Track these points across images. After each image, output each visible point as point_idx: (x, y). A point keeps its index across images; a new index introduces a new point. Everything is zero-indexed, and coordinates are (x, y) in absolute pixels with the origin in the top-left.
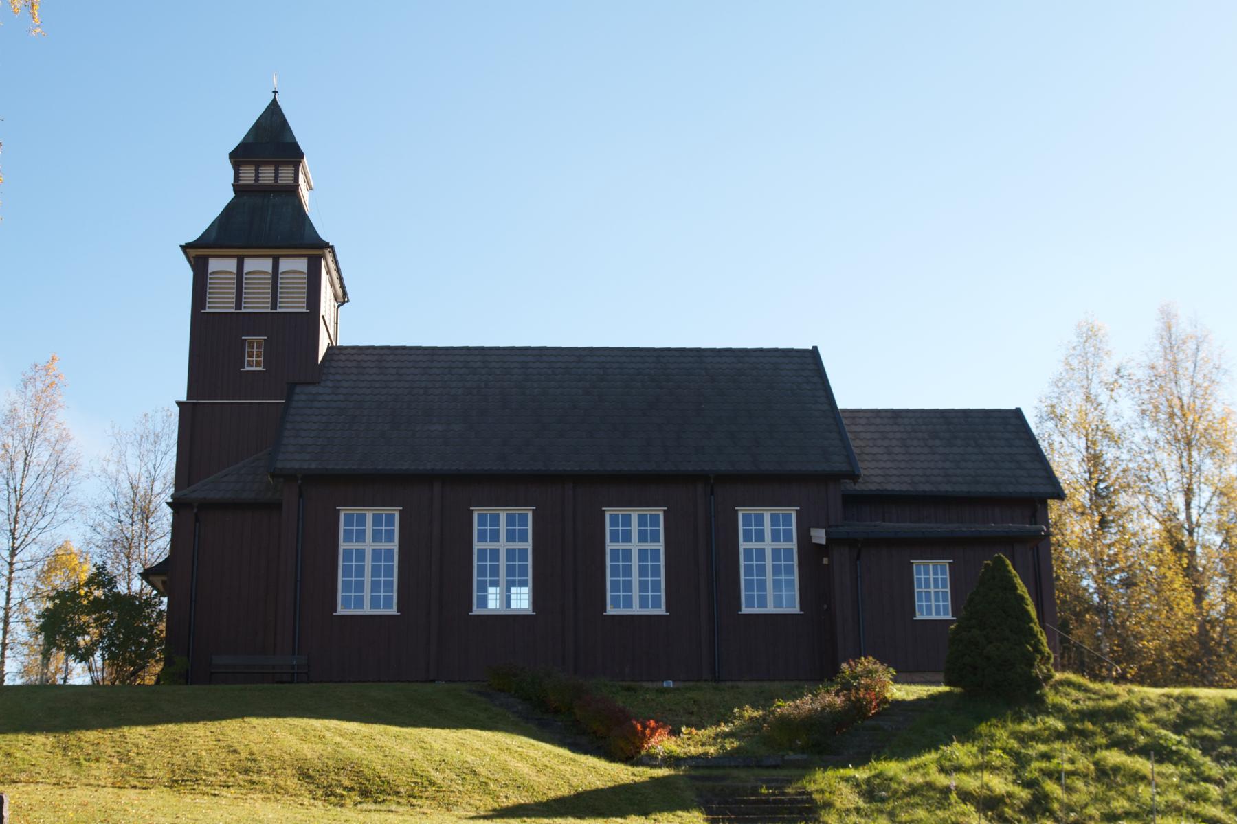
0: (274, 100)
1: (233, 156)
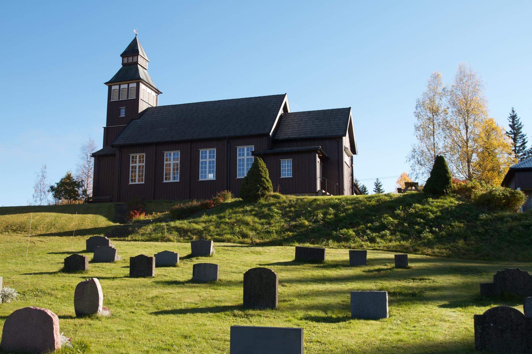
0: (136, 38)
1: (121, 55)
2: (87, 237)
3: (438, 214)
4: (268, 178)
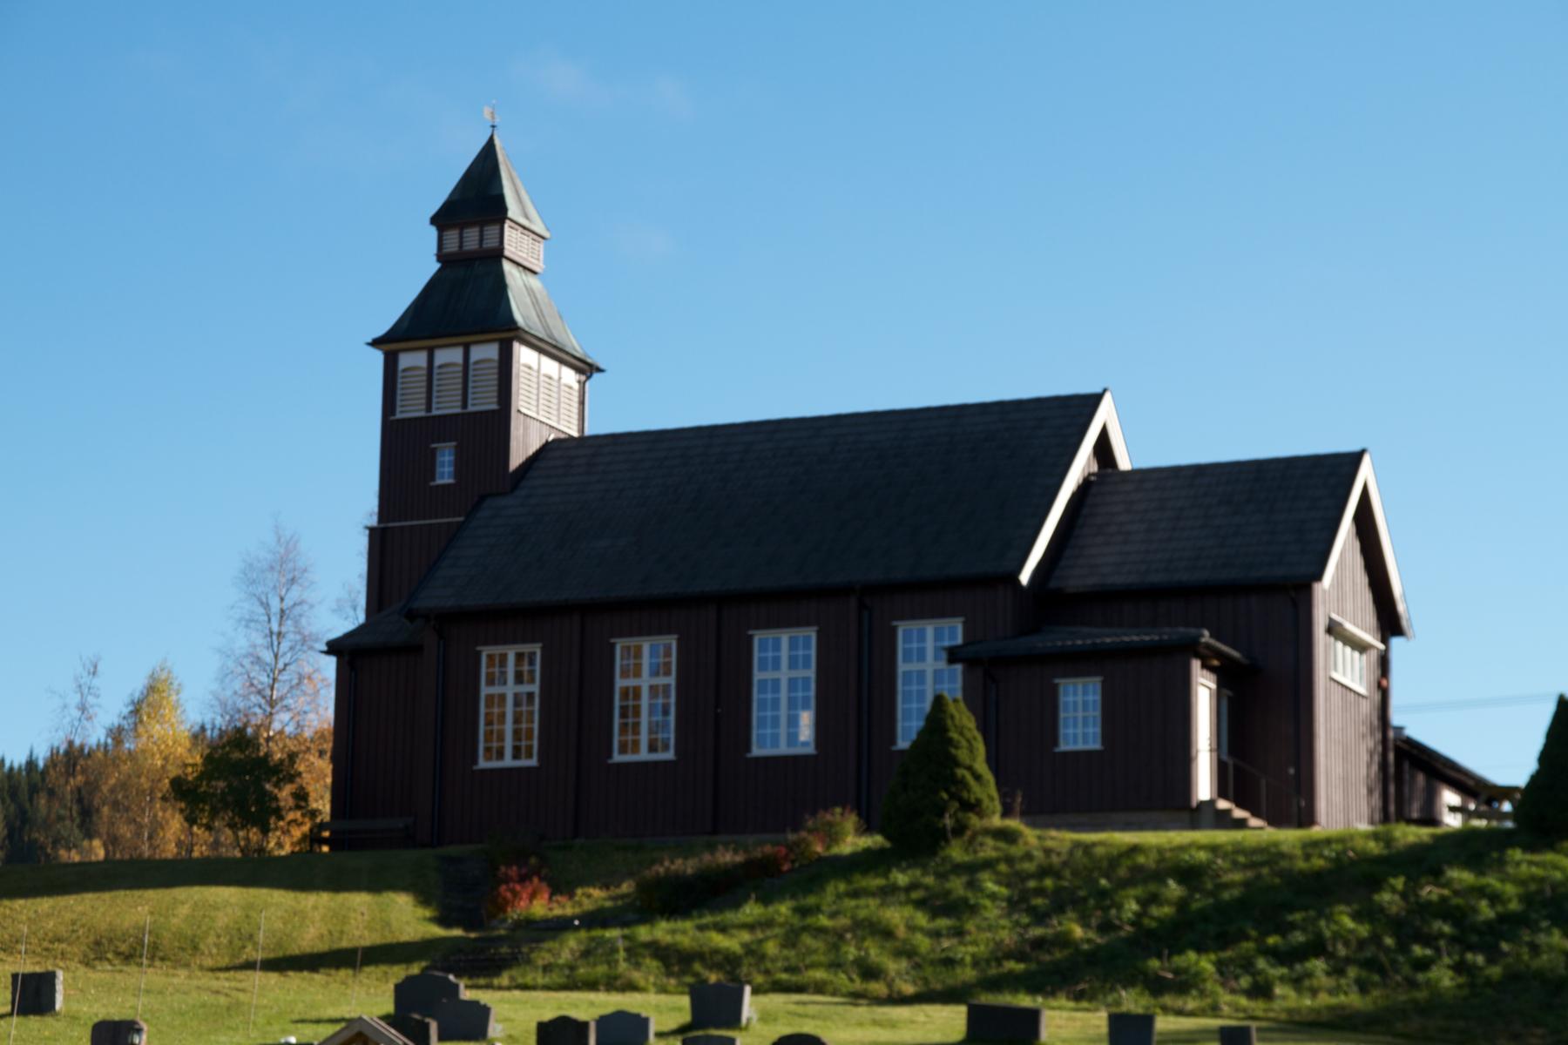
1: (435, 220)
2: (399, 973)
3: (1514, 906)
4: (981, 766)
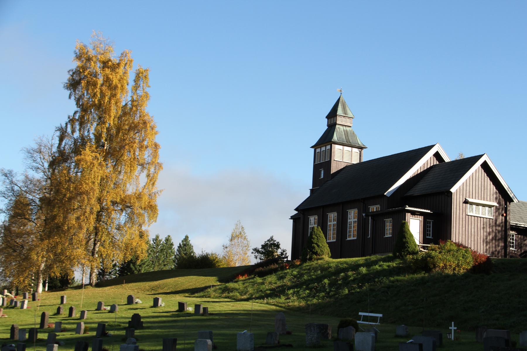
1: (326, 117)
